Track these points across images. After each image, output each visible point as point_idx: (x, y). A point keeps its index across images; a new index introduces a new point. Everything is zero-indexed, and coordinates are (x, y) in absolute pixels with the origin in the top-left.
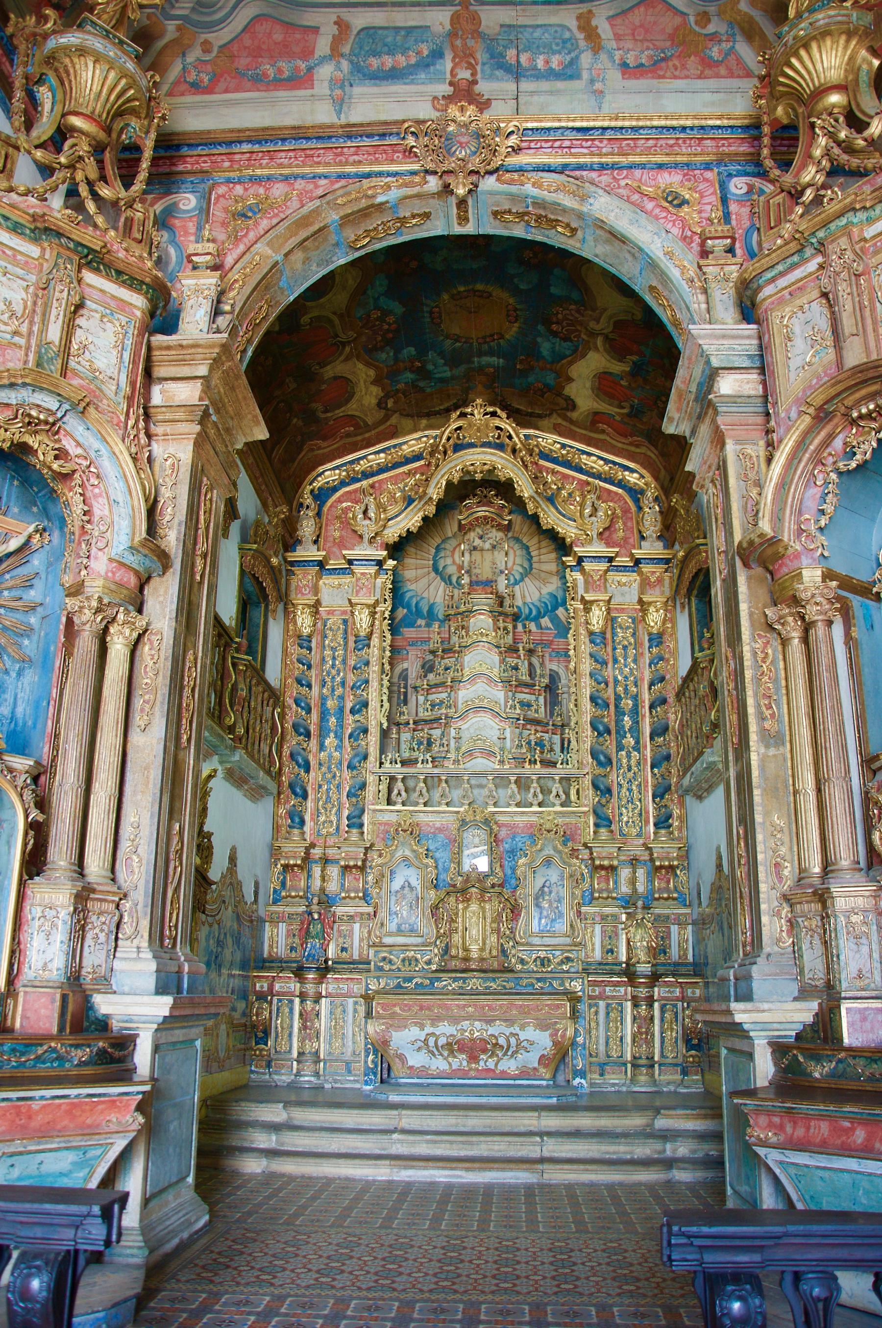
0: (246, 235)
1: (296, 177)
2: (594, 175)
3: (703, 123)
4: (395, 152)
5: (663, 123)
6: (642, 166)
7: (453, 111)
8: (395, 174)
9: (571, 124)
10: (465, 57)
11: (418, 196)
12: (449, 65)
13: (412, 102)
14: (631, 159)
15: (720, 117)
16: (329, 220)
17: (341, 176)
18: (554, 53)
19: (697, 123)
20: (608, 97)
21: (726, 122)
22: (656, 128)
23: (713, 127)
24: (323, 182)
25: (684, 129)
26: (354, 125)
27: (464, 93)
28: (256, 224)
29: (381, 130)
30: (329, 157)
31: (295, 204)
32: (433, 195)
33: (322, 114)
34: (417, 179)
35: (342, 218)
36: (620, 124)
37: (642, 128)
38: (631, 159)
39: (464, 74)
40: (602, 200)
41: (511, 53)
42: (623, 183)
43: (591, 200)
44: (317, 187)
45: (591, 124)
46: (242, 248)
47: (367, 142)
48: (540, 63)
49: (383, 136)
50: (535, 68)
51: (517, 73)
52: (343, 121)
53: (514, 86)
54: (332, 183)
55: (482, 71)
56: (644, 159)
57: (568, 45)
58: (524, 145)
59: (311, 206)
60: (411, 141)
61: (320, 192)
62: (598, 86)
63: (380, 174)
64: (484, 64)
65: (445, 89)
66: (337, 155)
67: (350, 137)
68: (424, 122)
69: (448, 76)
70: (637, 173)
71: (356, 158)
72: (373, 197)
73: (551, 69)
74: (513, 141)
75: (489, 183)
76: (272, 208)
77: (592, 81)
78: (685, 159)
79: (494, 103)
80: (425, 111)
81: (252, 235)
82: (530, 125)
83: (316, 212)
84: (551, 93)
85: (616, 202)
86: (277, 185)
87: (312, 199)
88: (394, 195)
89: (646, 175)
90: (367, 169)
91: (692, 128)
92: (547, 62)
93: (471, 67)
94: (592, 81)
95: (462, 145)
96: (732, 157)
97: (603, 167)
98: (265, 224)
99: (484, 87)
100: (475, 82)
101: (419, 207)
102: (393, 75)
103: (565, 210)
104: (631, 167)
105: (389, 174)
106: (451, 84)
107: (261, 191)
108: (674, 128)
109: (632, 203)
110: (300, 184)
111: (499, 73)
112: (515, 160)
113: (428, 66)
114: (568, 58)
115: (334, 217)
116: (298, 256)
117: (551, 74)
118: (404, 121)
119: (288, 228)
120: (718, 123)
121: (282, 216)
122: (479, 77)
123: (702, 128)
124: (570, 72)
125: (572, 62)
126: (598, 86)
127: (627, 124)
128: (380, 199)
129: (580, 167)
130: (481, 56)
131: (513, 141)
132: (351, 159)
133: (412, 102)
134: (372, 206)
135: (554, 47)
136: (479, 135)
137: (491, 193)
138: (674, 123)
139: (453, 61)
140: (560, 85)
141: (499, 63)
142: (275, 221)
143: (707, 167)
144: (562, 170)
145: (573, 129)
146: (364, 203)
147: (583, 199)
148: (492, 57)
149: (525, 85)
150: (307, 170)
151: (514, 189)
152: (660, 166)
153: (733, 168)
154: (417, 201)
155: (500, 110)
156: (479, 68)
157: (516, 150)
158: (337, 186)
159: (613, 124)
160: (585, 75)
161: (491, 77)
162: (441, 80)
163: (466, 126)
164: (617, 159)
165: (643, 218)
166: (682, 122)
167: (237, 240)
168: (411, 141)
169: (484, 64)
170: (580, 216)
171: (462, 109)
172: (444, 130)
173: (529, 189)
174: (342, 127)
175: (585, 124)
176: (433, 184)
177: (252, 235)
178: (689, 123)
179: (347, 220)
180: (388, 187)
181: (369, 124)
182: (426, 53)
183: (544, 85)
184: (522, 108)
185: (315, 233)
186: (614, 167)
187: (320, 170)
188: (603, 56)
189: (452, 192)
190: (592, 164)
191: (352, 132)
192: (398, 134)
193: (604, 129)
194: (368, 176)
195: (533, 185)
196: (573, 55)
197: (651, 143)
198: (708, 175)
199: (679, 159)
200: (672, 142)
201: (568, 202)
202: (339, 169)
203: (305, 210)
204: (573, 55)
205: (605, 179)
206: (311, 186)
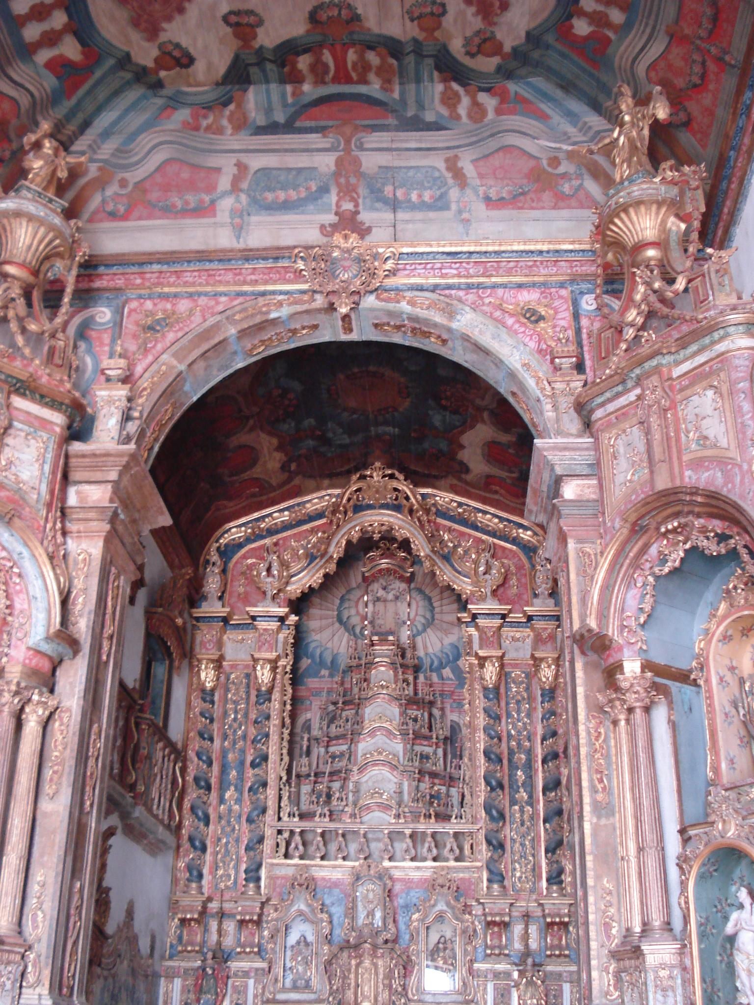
0: (154, 347)
1: (200, 294)
2: (461, 293)
3: (558, 247)
4: (287, 272)
5: (522, 247)
6: (504, 286)
7: (338, 239)
8: (287, 293)
9: (441, 249)
10: (348, 192)
11: (307, 312)
12: (334, 198)
13: (302, 229)
14: (494, 279)
15: (573, 242)
16: (228, 334)
17: (239, 294)
18: (426, 189)
19: (552, 247)
20: (474, 225)
21: (577, 247)
22: (517, 252)
23: (566, 251)
24: (223, 299)
25: (541, 252)
26: (251, 250)
27: (349, 223)
28: (164, 336)
29: (275, 253)
30: (230, 276)
31: (197, 318)
32: (319, 310)
33: (224, 239)
34: (306, 297)
35: (239, 332)
36: (484, 249)
37: (503, 252)
38: (494, 279)
39: (348, 206)
40: (469, 316)
41: (388, 190)
42: (487, 301)
43: (459, 317)
44: (218, 303)
45: (459, 249)
46: (150, 358)
47: (261, 264)
48: (414, 197)
49: (276, 259)
50: (409, 201)
51: (394, 205)
52: (242, 246)
53: (392, 216)
54: (232, 300)
55: (364, 204)
56: (505, 280)
57: (438, 183)
58: (400, 266)
59: (211, 321)
60: (301, 265)
61: (220, 308)
62: (465, 215)
63: (274, 293)
64: (365, 198)
65: (330, 218)
66: (236, 275)
67: (247, 259)
68: (313, 247)
69: (334, 207)
70: (500, 292)
71: (253, 277)
72: (268, 313)
73: (423, 202)
74: (389, 265)
75: (370, 301)
76: (178, 323)
77: (460, 212)
78: (542, 279)
79: (374, 230)
80: (312, 236)
81: (159, 347)
82: (405, 250)
83: (217, 327)
84: (423, 221)
85: (480, 319)
86: (183, 301)
87: (213, 315)
88: (285, 312)
89: (508, 295)
90: (262, 288)
91: (548, 252)
92: (420, 196)
93: (353, 200)
94: (460, 212)
95: (345, 269)
96: (584, 278)
97: (469, 287)
98: (171, 336)
99: (365, 217)
100: (357, 213)
101: (308, 321)
102: (286, 206)
103: (435, 325)
104: (494, 286)
105: (281, 293)
106: (336, 214)
107: (169, 306)
108: (532, 252)
109: (496, 320)
110: (203, 301)
111: (378, 205)
112: (391, 282)
113: (316, 199)
114: (438, 193)
115: (233, 331)
116: (201, 364)
117: (423, 206)
118: (295, 247)
119: (191, 341)
120: (571, 247)
121: (187, 329)
122: (361, 208)
123: (557, 251)
124: (440, 204)
125: (441, 196)
126: (465, 215)
127: (490, 249)
128: (273, 315)
129: (450, 287)
130: (362, 191)
131: (389, 265)
132: (249, 278)
133: (302, 229)
134: (267, 321)
135: (426, 184)
136: (360, 260)
137: (372, 310)
138: (532, 247)
139: (338, 195)
140: (432, 215)
141: (377, 195)
142: (180, 334)
143: (562, 285)
144: (435, 288)
145: (443, 253)
146: (258, 319)
147: (451, 315)
148: (372, 192)
149: (401, 215)
150: (209, 289)
151: (391, 306)
152: (520, 286)
153: (585, 286)
154: (305, 316)
155: (379, 237)
156: (360, 201)
157: (393, 273)
158: (235, 303)
159: (478, 249)
160: (454, 207)
161: (373, 209)
162: (327, 211)
163: (349, 251)
164: (482, 280)
165: (503, 333)
166: (539, 247)
167: (146, 351)
168: (301, 265)
169: (365, 198)
170: (449, 330)
171: (346, 237)
172: (330, 255)
173: (404, 306)
174: (240, 251)
175: (453, 249)
176: (320, 301)
177: (159, 347)
178: (545, 248)
179: (243, 334)
180: (280, 304)
181: (265, 249)
182: (314, 188)
183: (419, 215)
184: (399, 234)
185: (216, 345)
186: (479, 286)
187: (221, 289)
188: (468, 191)
189: (335, 309)
190: (460, 284)
191: (249, 255)
192: (290, 257)
193: (471, 253)
194: (263, 294)
195: (408, 303)
196: (442, 190)
197: (512, 265)
198: (563, 292)
199: (536, 279)
200: (531, 263)
201: (438, 318)
202: (238, 288)
203: (208, 324)
204: (442, 190)
205: (471, 297)
206: (212, 303)
